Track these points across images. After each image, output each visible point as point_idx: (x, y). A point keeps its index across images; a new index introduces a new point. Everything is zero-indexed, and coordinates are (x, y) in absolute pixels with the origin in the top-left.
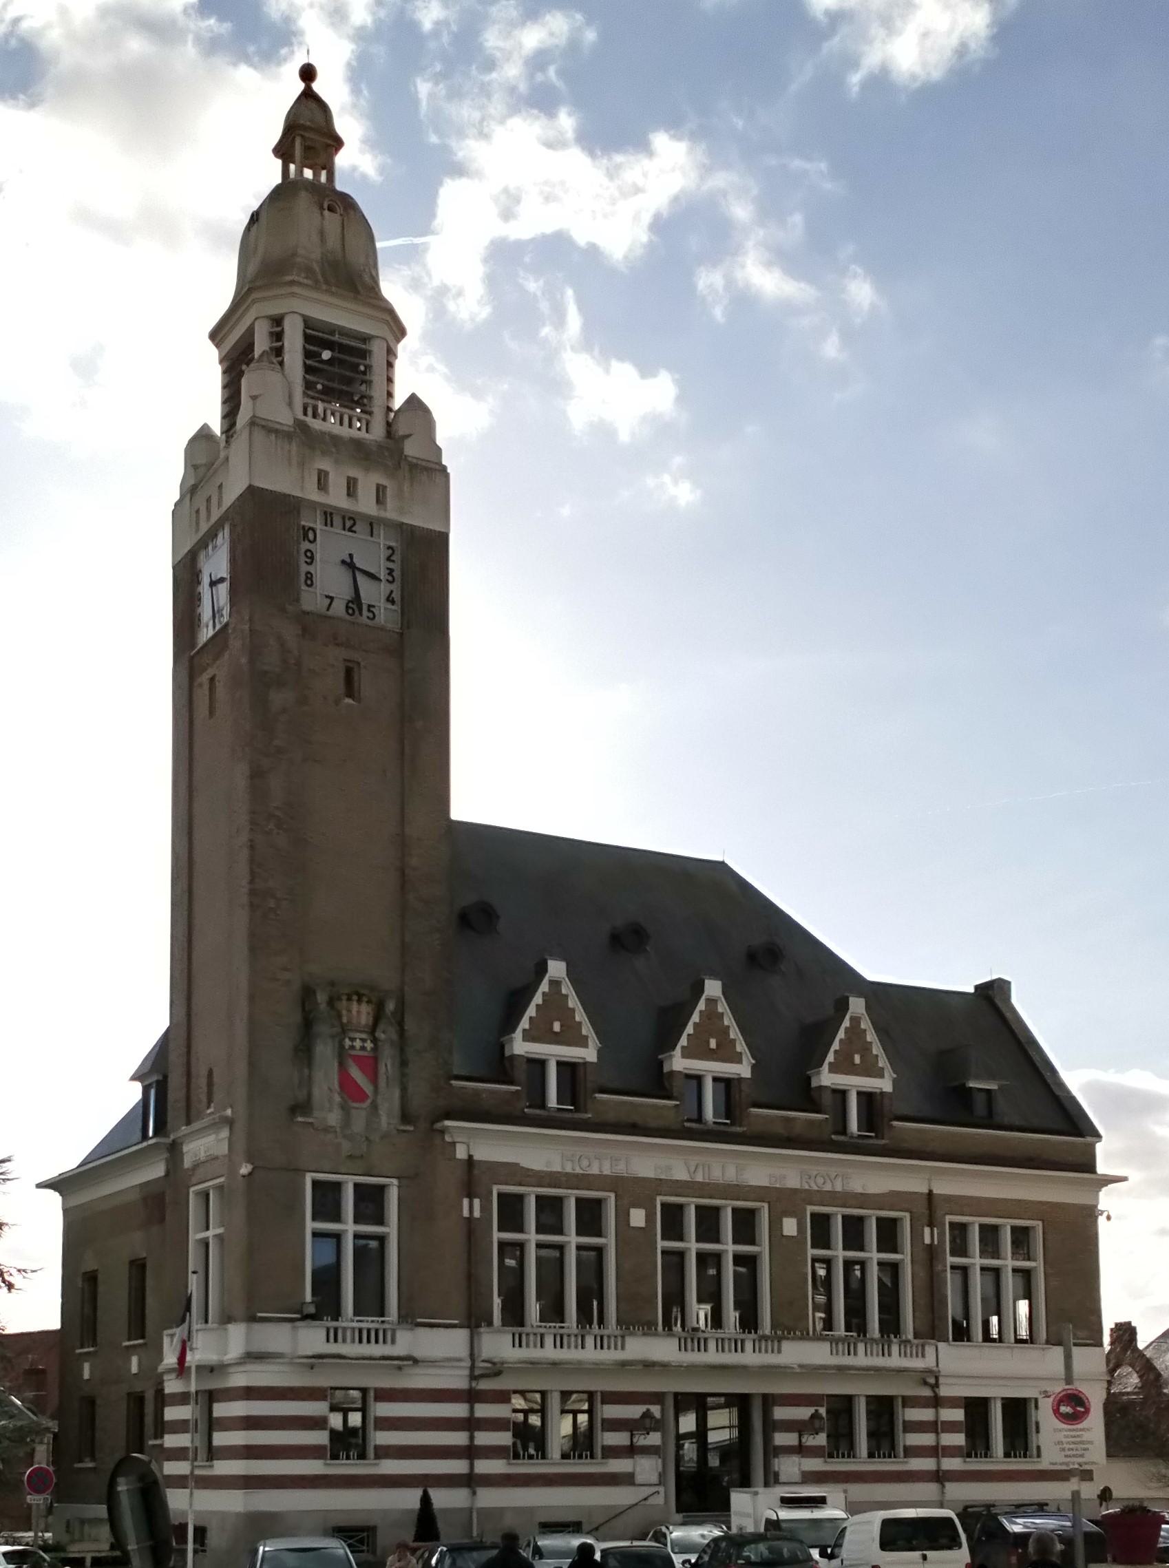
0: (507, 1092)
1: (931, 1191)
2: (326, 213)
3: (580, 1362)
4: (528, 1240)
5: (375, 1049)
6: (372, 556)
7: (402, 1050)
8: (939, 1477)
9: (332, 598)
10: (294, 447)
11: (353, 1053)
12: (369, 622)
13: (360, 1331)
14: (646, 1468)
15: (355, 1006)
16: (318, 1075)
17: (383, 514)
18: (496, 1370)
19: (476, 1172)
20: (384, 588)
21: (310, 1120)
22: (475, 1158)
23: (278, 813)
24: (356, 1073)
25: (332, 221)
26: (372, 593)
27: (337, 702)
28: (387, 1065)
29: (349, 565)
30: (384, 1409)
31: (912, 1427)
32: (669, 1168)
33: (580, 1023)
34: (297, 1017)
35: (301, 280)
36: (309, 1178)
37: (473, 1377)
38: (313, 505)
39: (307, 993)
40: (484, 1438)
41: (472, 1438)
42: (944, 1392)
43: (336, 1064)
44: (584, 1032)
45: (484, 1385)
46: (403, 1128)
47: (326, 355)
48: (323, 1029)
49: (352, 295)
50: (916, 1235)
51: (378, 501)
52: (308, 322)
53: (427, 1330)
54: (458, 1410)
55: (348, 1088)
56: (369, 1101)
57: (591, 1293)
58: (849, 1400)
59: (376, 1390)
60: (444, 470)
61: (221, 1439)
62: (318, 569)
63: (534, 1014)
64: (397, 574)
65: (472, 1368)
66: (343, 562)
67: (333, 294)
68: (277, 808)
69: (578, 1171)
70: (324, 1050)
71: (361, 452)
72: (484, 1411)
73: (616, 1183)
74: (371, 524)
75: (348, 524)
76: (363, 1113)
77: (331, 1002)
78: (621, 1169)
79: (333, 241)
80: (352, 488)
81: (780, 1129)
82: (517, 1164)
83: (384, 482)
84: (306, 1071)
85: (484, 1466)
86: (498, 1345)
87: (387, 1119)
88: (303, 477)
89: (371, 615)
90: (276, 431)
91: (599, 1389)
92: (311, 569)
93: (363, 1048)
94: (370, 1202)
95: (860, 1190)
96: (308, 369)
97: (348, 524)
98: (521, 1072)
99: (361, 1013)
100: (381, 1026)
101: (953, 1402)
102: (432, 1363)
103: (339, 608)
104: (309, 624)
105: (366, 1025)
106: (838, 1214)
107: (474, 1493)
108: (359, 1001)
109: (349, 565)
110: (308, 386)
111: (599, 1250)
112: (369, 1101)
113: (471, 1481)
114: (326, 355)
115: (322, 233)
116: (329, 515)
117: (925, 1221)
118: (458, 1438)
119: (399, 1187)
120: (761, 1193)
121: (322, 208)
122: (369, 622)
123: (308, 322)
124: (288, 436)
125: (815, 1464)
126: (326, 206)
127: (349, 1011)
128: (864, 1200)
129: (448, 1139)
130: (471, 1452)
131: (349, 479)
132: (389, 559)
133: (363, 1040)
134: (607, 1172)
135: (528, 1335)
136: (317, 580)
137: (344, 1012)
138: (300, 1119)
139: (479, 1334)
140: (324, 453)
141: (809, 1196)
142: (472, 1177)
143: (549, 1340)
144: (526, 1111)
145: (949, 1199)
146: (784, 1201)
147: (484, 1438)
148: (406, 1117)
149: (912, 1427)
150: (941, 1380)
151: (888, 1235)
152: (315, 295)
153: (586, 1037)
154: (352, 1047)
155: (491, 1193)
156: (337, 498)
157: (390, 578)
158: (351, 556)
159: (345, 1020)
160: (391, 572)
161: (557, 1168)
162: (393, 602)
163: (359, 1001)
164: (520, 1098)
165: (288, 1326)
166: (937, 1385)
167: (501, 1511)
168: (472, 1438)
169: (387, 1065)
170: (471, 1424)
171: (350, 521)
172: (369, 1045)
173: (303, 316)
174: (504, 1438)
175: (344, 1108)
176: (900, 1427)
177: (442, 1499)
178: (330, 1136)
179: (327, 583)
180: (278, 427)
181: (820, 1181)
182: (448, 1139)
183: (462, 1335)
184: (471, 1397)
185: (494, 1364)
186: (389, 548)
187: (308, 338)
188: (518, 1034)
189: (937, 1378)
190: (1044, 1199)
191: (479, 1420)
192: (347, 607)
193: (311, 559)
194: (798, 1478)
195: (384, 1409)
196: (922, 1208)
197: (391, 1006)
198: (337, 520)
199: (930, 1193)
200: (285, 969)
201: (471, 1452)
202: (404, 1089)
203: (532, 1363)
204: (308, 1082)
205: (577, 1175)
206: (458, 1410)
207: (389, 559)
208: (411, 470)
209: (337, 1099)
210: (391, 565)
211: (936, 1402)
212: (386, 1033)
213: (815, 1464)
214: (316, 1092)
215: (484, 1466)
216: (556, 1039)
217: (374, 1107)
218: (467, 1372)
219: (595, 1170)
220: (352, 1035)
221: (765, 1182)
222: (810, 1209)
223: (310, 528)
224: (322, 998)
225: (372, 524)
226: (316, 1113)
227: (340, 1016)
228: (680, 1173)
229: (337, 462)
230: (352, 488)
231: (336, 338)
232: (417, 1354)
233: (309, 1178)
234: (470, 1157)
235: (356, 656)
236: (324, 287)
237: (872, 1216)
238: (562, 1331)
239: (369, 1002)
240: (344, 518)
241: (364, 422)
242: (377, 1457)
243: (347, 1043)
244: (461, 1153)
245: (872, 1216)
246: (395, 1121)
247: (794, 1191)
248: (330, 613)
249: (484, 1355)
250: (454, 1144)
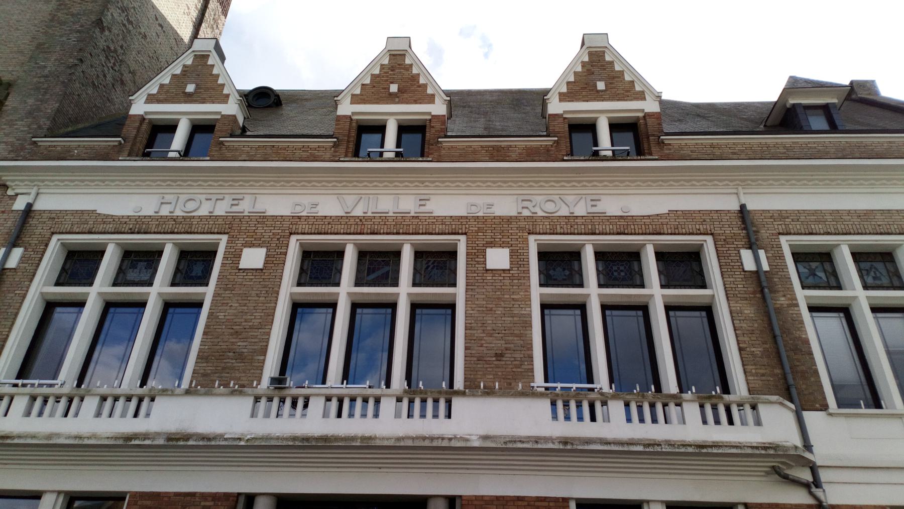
1: (743, 207)
50: (729, 265)
69: (178, 213)
73: (231, 225)
120: (457, 225)
128: (625, 225)
141: (532, 225)
145: (782, 215)
150: (824, 476)
151: (682, 266)
166: (817, 483)
182: (10, 192)
199: (743, 207)
205: (175, 219)
244: (20, 205)
247: (509, 220)
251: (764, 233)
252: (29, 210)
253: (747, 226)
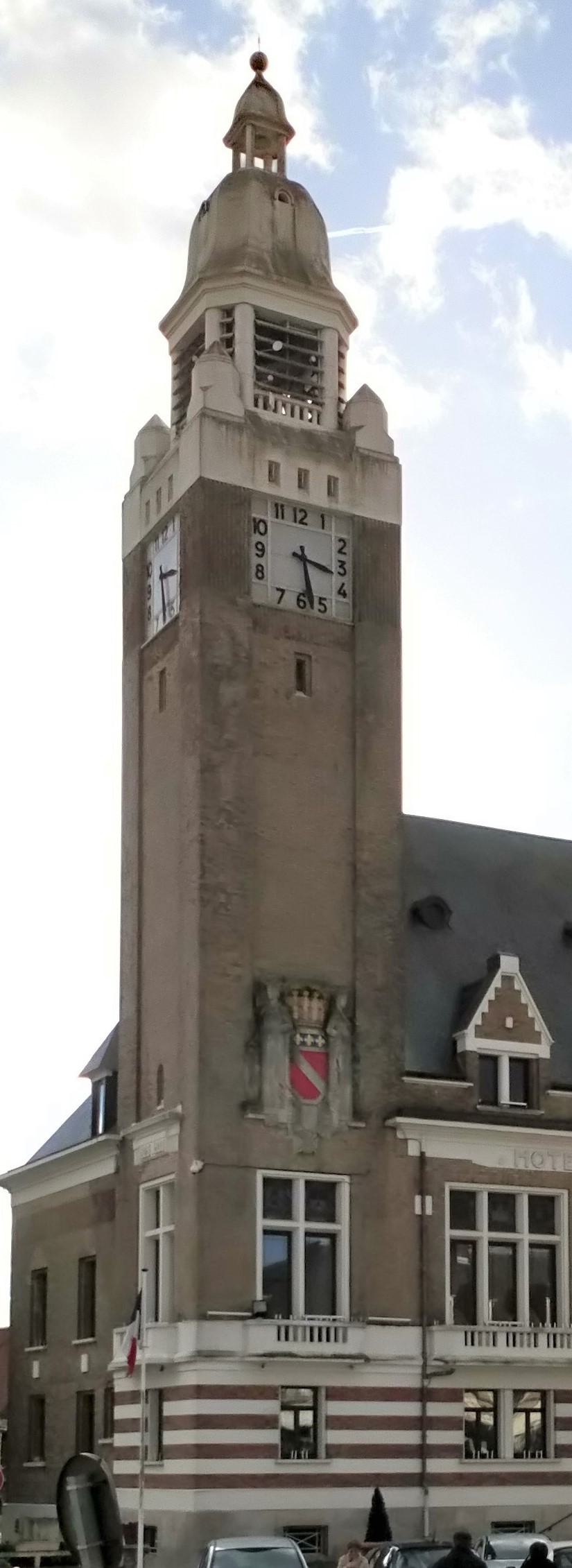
0: (459, 1089)
2: (277, 202)
3: (533, 1361)
4: (481, 1238)
5: (327, 1045)
6: (324, 549)
7: (353, 1046)
9: (283, 591)
10: (245, 439)
11: (305, 1049)
12: (321, 615)
13: (312, 1329)
15: (306, 1002)
16: (269, 1071)
17: (334, 506)
18: (449, 1369)
19: (428, 1169)
20: (336, 581)
21: (261, 1117)
22: (428, 1154)
23: (228, 807)
24: (307, 1069)
25: (283, 211)
26: (323, 585)
27: (288, 695)
28: (339, 1061)
29: (301, 557)
30: (335, 1408)
33: (533, 1019)
34: (248, 1014)
35: (252, 270)
36: (260, 1175)
37: (425, 1376)
38: (264, 497)
39: (258, 989)
40: (436, 1437)
41: (424, 1437)
43: (287, 1060)
44: (537, 1028)
45: (436, 1384)
46: (354, 1124)
47: (277, 346)
48: (274, 1025)
49: (303, 285)
51: (329, 493)
52: (259, 313)
53: (379, 1328)
54: (410, 1409)
55: (298, 1081)
56: (320, 1098)
57: (543, 1292)
59: (327, 1389)
60: (395, 461)
62: (268, 562)
63: (486, 1010)
64: (348, 566)
65: (424, 1366)
66: (295, 554)
67: (283, 284)
68: (228, 802)
69: (531, 1168)
70: (275, 1046)
71: (312, 444)
72: (436, 1409)
74: (322, 516)
75: (300, 516)
76: (314, 1110)
77: (282, 998)
79: (284, 231)
80: (302, 480)
82: (469, 1161)
83: (335, 474)
84: (257, 1067)
85: (436, 1466)
86: (450, 1342)
87: (339, 1115)
88: (254, 469)
89: (322, 608)
90: (227, 423)
91: (552, 1388)
92: (262, 561)
93: (314, 1044)
94: (322, 1199)
96: (259, 360)
97: (300, 516)
98: (473, 1068)
99: (313, 1009)
100: (333, 1022)
102: (384, 1361)
103: (290, 601)
104: (259, 618)
105: (318, 1021)
107: (426, 1493)
108: (310, 996)
109: (301, 557)
110: (259, 377)
111: (552, 1248)
112: (320, 1098)
113: (422, 1480)
114: (277, 346)
115: (273, 223)
116: (279, 508)
118: (410, 1437)
119: (351, 1184)
121: (273, 198)
122: (321, 615)
123: (259, 313)
124: (239, 428)
126: (277, 196)
127: (301, 1007)
129: (400, 1135)
130: (422, 1452)
131: (300, 471)
132: (340, 551)
133: (315, 1036)
135: (480, 1333)
136: (268, 572)
137: (295, 1008)
138: (251, 1116)
139: (431, 1332)
140: (274, 444)
142: (424, 1173)
143: (501, 1339)
144: (480, 1109)
147: (436, 1437)
148: (357, 1114)
152: (265, 285)
153: (539, 1033)
154: (303, 1043)
155: (443, 1190)
156: (287, 490)
157: (342, 571)
158: (302, 548)
159: (296, 1016)
160: (342, 564)
161: (509, 1165)
162: (344, 595)
163: (310, 996)
164: (473, 1095)
165: (239, 1324)
167: (454, 1511)
168: (424, 1437)
169: (339, 1061)
170: (423, 1423)
171: (301, 514)
172: (320, 1041)
173: (254, 306)
174: (457, 1437)
175: (296, 1105)
177: (394, 1498)
178: (281, 1133)
179: (279, 576)
180: (229, 418)
182: (400, 1135)
183: (415, 1332)
184: (424, 1395)
185: (446, 1362)
186: (341, 540)
187: (259, 329)
188: (470, 1030)
191: (431, 1419)
192: (299, 600)
193: (262, 551)
195: (335, 1408)
197: (342, 1002)
198: (288, 512)
200: (236, 965)
201: (422, 1452)
202: (355, 1086)
203: (485, 1362)
204: (258, 1079)
205: (530, 1173)
206: (410, 1409)
207: (340, 551)
208: (362, 462)
209: (288, 1095)
210: (342, 558)
212: (338, 1029)
214: (267, 1088)
215: (436, 1466)
216: (509, 1035)
217: (326, 1103)
218: (419, 1371)
219: (548, 1167)
220: (303, 1031)
223: (261, 521)
224: (272, 993)
225: (323, 517)
226: (267, 1110)
227: (291, 1012)
229: (288, 453)
230: (302, 480)
231: (287, 329)
232: (369, 1352)
233: (260, 1175)
234: (422, 1154)
235: (306, 649)
236: (275, 277)
238: (514, 1329)
239: (320, 998)
240: (295, 510)
241: (315, 413)
242: (328, 1456)
243: (299, 1039)
244: (413, 1150)
246: (347, 1117)
248: (281, 606)
249: (437, 1354)
250: (406, 1140)
252: (422, 1158)
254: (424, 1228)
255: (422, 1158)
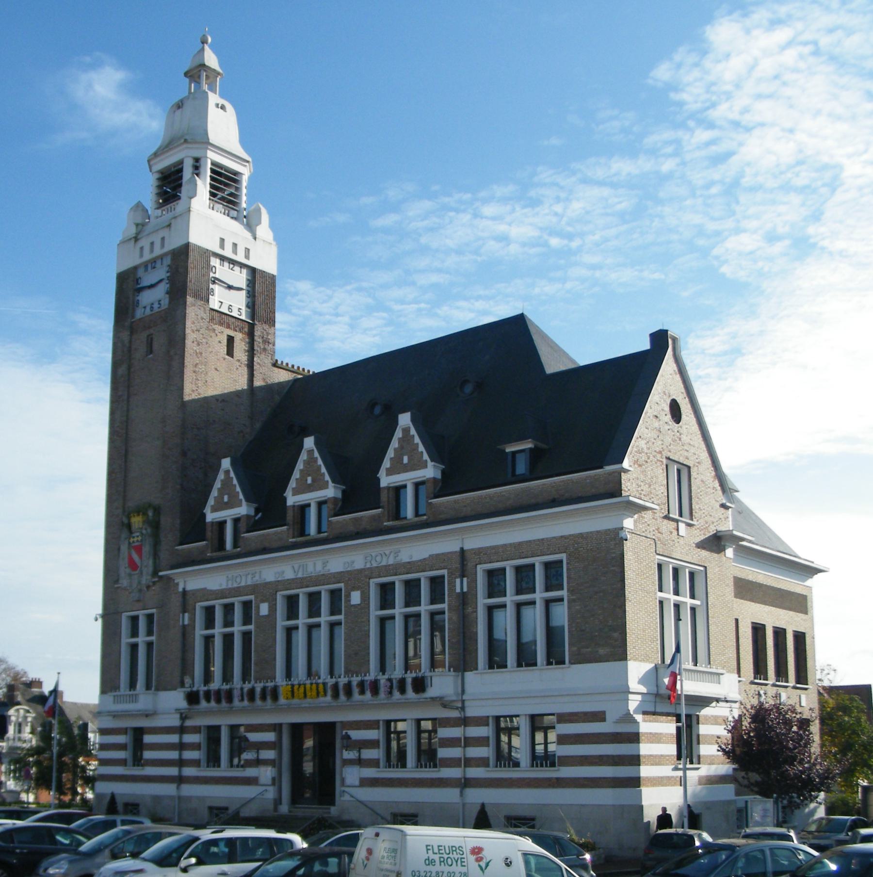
1: (462, 549)
8: (466, 783)
14: (266, 773)
19: (188, 597)
31: (196, 747)
32: (283, 572)
40: (188, 755)
41: (180, 755)
42: (471, 712)
45: (189, 723)
58: (217, 728)
61: (148, 755)
73: (254, 589)
76: (136, 577)
78: (257, 579)
81: (351, 528)
82: (205, 589)
85: (188, 771)
95: (408, 560)
101: (482, 721)
106: (398, 581)
113: (180, 780)
117: (457, 574)
125: (370, 773)
128: (410, 567)
130: (181, 763)
134: (249, 583)
142: (186, 599)
144: (218, 552)
145: (479, 551)
146: (356, 579)
147: (188, 755)
149: (196, 747)
150: (467, 704)
166: (463, 708)
170: (181, 747)
176: (204, 746)
181: (379, 559)
184: (182, 730)
189: (463, 701)
190: (566, 533)
194: (357, 783)
196: (457, 565)
199: (462, 549)
201: (181, 763)
205: (234, 589)
211: (465, 722)
213: (370, 773)
215: (188, 771)
221: (340, 569)
222: (373, 582)
228: (289, 575)
237: (424, 577)
245: (424, 577)
246: (149, 577)
247: (360, 571)
251: (470, 565)
252: (185, 592)
253: (463, 561)
254: (186, 633)
255: (185, 592)
